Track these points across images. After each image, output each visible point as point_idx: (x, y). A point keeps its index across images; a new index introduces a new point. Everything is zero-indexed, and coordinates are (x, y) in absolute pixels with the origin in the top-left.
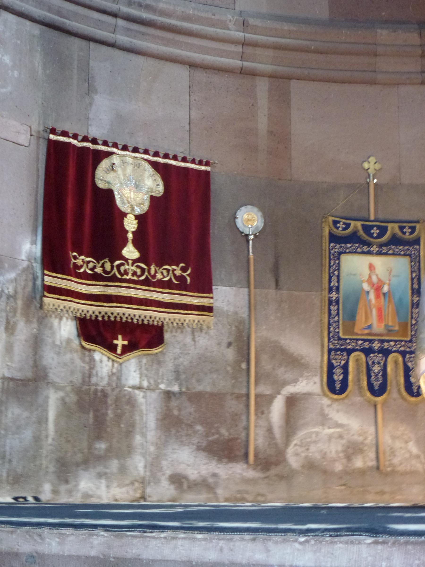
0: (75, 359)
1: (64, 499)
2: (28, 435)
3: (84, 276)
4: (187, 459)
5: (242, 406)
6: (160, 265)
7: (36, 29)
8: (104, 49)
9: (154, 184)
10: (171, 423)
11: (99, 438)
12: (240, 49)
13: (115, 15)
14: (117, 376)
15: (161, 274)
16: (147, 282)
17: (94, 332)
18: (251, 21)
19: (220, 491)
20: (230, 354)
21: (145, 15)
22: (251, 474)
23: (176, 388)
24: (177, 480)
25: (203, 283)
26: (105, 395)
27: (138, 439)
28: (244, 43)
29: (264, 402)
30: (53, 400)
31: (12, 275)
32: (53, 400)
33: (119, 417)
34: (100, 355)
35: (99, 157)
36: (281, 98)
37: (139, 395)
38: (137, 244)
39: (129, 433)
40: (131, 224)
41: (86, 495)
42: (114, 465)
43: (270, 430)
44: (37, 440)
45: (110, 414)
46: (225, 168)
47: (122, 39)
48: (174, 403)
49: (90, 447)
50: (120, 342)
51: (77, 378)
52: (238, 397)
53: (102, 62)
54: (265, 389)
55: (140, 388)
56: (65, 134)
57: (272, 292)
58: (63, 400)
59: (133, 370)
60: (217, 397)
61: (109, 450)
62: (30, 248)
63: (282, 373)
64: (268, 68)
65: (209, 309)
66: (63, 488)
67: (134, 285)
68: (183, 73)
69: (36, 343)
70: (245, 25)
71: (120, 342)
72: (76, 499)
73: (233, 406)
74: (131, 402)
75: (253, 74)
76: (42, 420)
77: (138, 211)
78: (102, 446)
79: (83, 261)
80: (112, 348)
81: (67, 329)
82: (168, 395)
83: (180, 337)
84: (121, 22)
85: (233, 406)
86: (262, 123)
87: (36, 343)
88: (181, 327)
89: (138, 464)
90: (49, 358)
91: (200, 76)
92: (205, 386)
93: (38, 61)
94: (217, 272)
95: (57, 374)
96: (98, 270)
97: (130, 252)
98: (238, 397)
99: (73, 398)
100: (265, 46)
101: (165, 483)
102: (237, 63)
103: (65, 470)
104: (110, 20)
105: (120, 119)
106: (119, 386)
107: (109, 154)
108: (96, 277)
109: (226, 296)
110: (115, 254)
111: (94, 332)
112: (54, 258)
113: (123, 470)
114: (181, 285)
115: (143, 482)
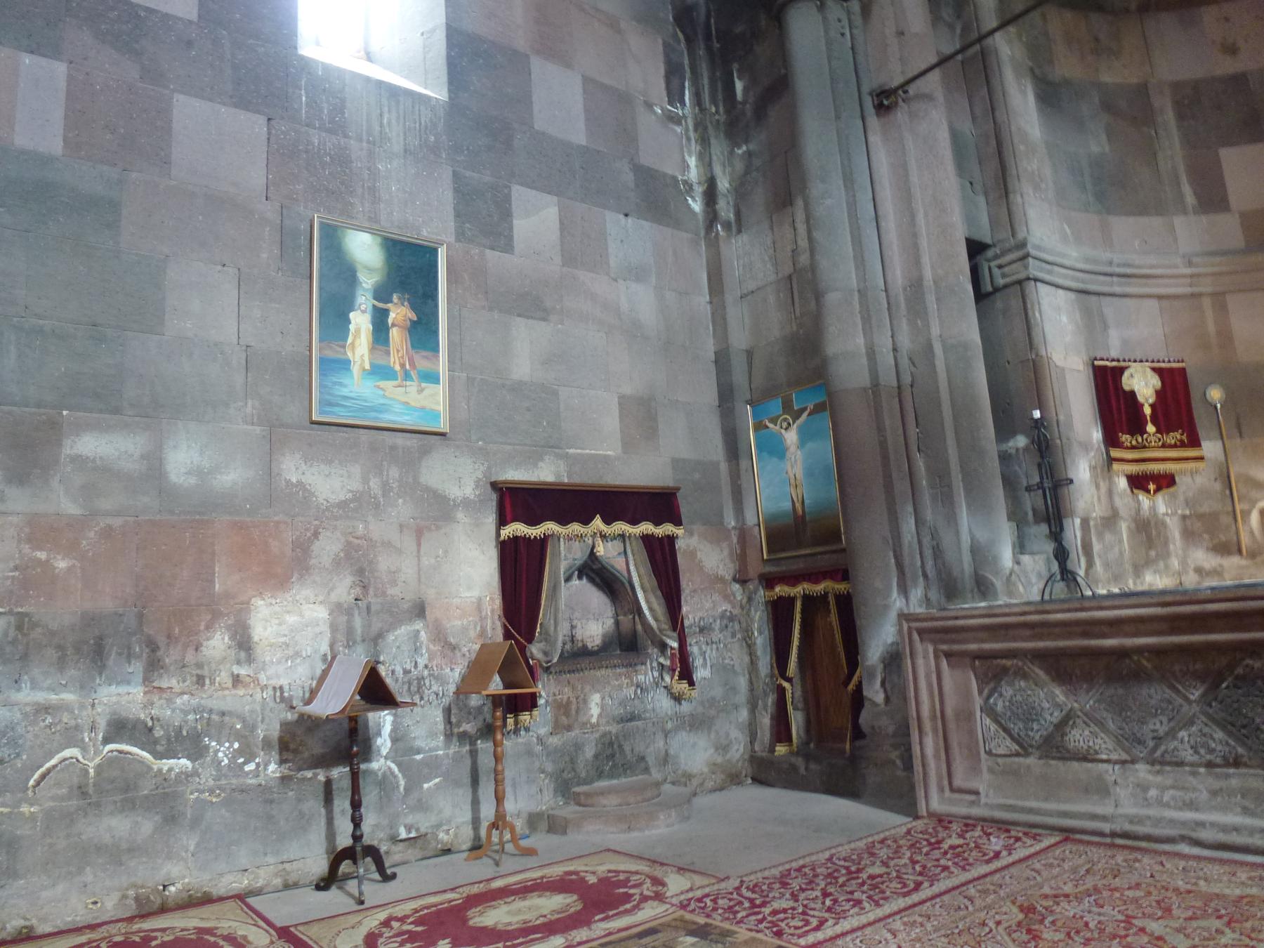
0: (1128, 499)
1: (1140, 588)
2: (1116, 550)
3: (1127, 448)
4: (1202, 557)
5: (1230, 519)
6: (1168, 433)
7: (1072, 295)
8: (1108, 299)
9: (1156, 382)
10: (1189, 535)
11: (1150, 548)
12: (1189, 280)
13: (1111, 275)
14: (1153, 508)
15: (1172, 438)
16: (1164, 446)
17: (1138, 482)
18: (1195, 260)
19: (1227, 576)
20: (1218, 486)
21: (1129, 271)
22: (1244, 562)
23: (1188, 512)
24: (1199, 570)
25: (1194, 442)
26: (1149, 522)
27: (1171, 547)
28: (1192, 276)
29: (1246, 514)
30: (1124, 527)
31: (1092, 454)
32: (1124, 527)
33: (1159, 534)
34: (1142, 497)
35: (1121, 370)
36: (1221, 307)
37: (1168, 519)
38: (1154, 423)
39: (1166, 543)
40: (1147, 411)
41: (1150, 585)
42: (1161, 564)
43: (1252, 532)
44: (1121, 553)
45: (1154, 532)
46: (1192, 362)
47: (1117, 289)
48: (1188, 522)
49: (1147, 554)
50: (1152, 487)
51: (1133, 513)
52: (1228, 513)
53: (1109, 308)
54: (1245, 506)
55: (1167, 514)
56: (1102, 359)
57: (1238, 440)
58: (1129, 527)
59: (1158, 504)
60: (1214, 516)
61: (1157, 555)
62: (1097, 435)
63: (1254, 494)
64: (1209, 289)
65: (1202, 458)
66: (1138, 581)
67: (1156, 449)
68: (1154, 303)
69: (1110, 493)
70: (1190, 264)
71: (1152, 487)
72: (1145, 587)
73: (1226, 520)
74: (1164, 524)
75: (1200, 295)
76: (1121, 541)
77: (1151, 401)
78: (1153, 553)
79: (1125, 438)
80: (1148, 491)
81: (1122, 483)
82: (1184, 517)
83: (1184, 479)
84: (1115, 279)
85: (1226, 520)
86: (1211, 328)
87: (1110, 493)
88: (1182, 472)
89: (1175, 563)
90: (1118, 502)
91: (1165, 303)
92: (1205, 508)
93: (1078, 316)
94: (1201, 433)
95: (1123, 512)
96: (1134, 443)
97: (1151, 428)
98: (1228, 513)
99: (1133, 525)
100: (1206, 275)
101: (1191, 573)
102: (1188, 290)
103: (1138, 570)
104: (1108, 279)
105: (1125, 343)
106: (1155, 514)
107: (1127, 368)
108: (1133, 448)
109: (1210, 448)
110: (1142, 431)
111: (1138, 482)
112: (1111, 440)
113: (1167, 567)
114: (1182, 445)
115: (1179, 574)
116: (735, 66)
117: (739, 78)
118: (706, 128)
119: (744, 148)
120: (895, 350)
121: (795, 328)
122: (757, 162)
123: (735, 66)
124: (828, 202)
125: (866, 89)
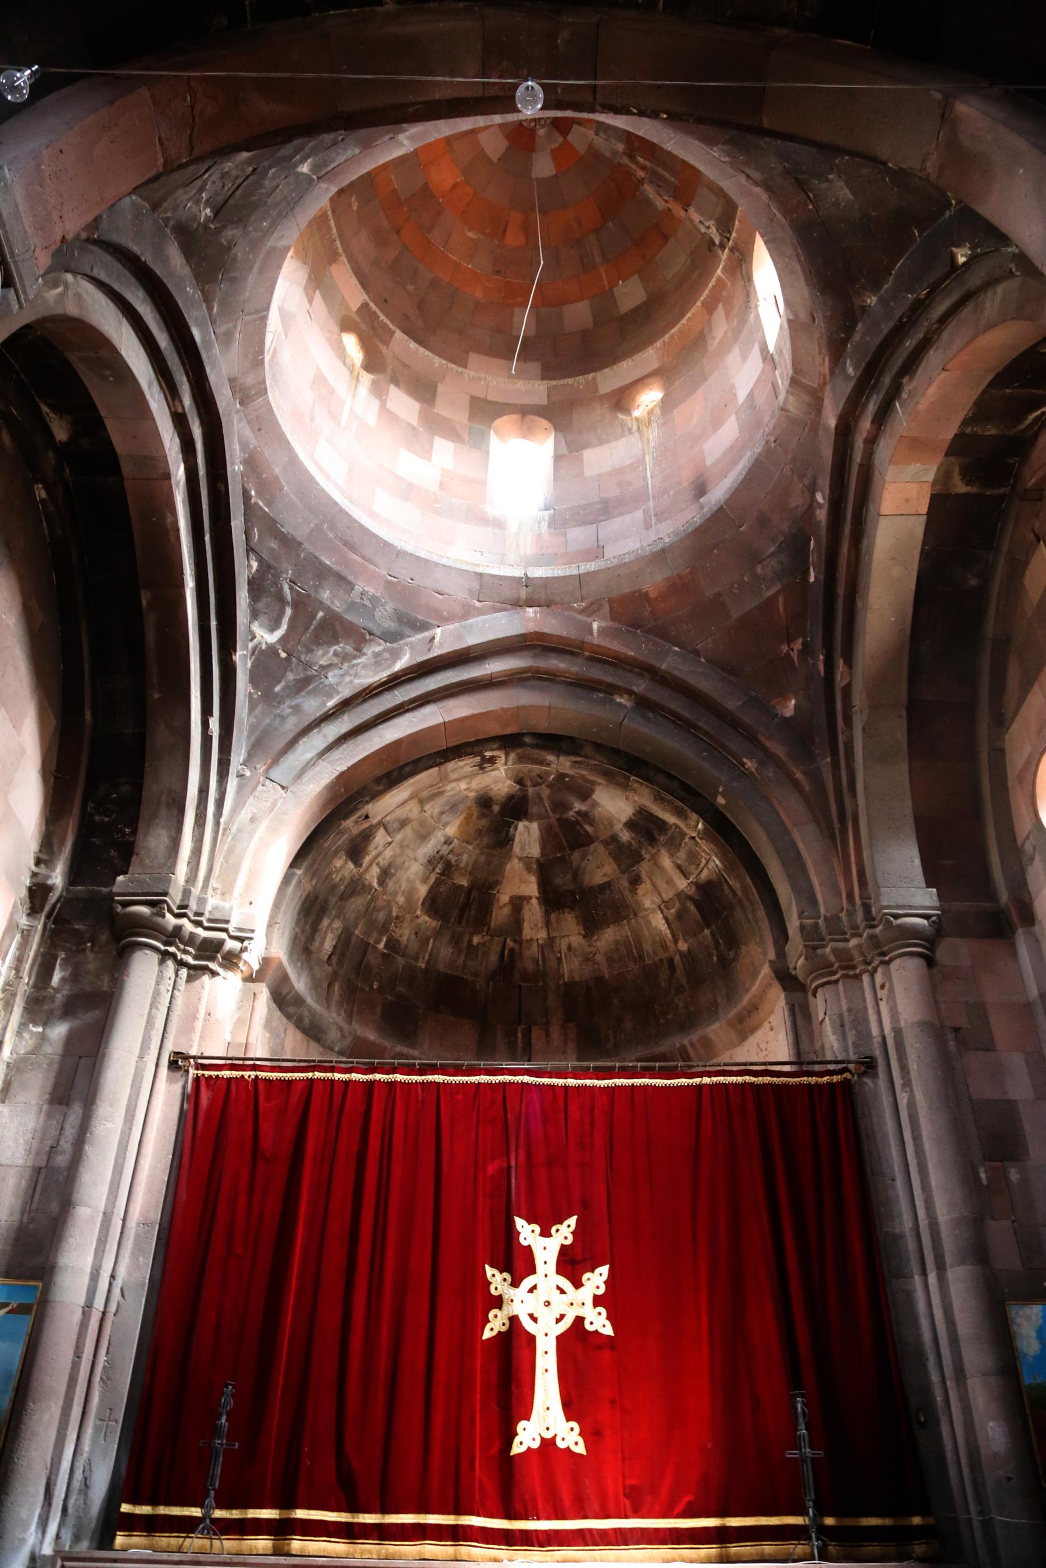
116: (62, 955)
117: (62, 969)
118: (14, 995)
119: (40, 1029)
120: (113, 1277)
121: (25, 1220)
122: (48, 1049)
123: (62, 955)
124: (109, 1125)
125: (170, 1047)
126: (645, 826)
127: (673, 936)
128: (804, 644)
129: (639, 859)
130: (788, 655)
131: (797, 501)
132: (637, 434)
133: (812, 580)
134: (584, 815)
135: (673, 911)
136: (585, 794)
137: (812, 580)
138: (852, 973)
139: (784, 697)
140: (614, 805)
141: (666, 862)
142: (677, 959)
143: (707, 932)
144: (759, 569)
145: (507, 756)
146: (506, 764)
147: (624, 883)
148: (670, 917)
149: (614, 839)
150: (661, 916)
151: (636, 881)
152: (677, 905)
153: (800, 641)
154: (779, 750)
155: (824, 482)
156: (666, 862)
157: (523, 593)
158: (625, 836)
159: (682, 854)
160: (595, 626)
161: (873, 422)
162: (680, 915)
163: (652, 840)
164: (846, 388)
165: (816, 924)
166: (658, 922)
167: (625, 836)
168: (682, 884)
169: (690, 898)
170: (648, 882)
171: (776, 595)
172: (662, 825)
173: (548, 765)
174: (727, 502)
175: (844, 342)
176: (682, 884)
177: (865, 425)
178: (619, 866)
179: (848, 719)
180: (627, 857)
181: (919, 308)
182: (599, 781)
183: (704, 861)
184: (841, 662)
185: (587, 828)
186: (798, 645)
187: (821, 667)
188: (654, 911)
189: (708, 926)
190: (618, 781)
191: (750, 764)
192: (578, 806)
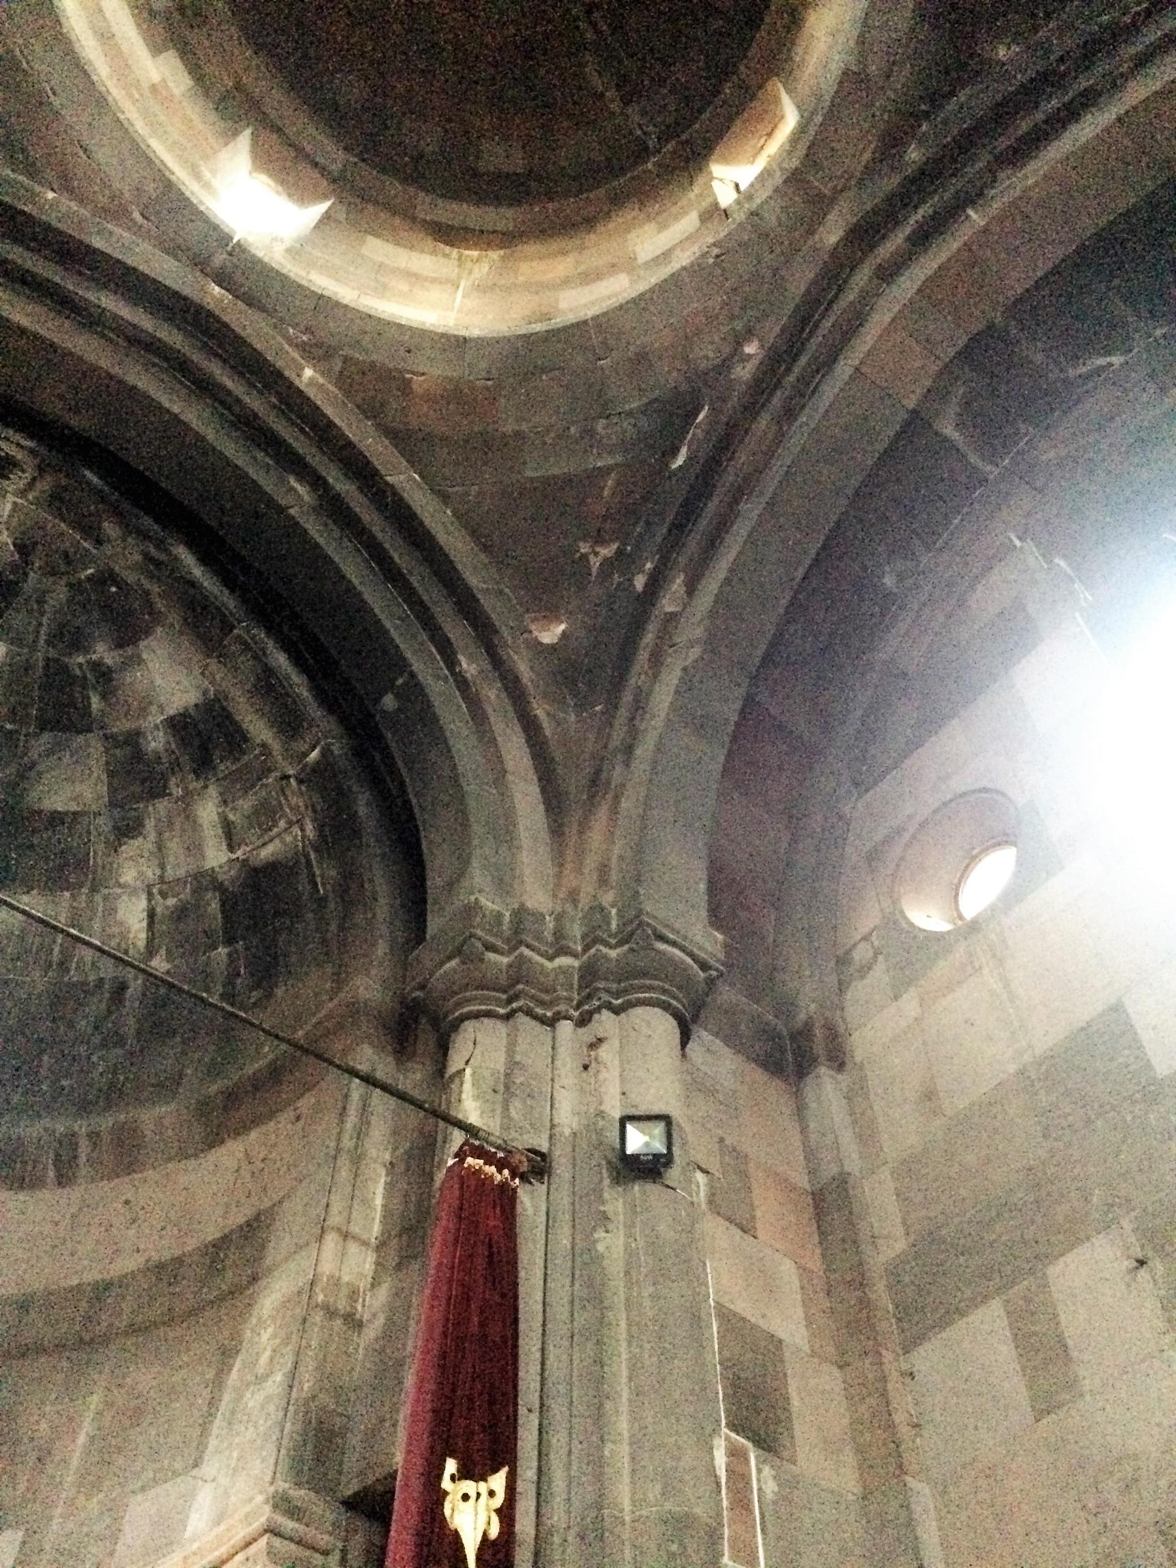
126: (206, 738)
127: (150, 941)
128: (620, 553)
129: (157, 791)
130: (584, 557)
131: (707, 352)
132: (456, 263)
133: (680, 461)
134: (104, 675)
135: (171, 901)
136: (128, 631)
137: (680, 461)
138: (539, 1011)
139: (551, 613)
140: (167, 679)
141: (208, 811)
142: (136, 985)
143: (222, 951)
144: (600, 425)
145: (41, 469)
146: (23, 493)
147: (104, 824)
148: (159, 910)
149: (133, 739)
150: (143, 903)
151: (127, 829)
152: (186, 894)
153: (615, 546)
154: (523, 668)
155: (773, 329)
156: (208, 811)
157: (219, 259)
158: (157, 742)
159: (246, 804)
160: (308, 373)
161: (908, 239)
162: (181, 913)
163: (203, 765)
164: (891, 183)
165: (499, 915)
166: (133, 917)
167: (157, 742)
168: (216, 856)
169: (219, 887)
170: (152, 837)
171: (608, 470)
172: (237, 740)
173: (99, 542)
174: (595, 318)
175: (919, 116)
176: (216, 856)
177: (896, 241)
178: (112, 790)
179: (656, 660)
180: (138, 779)
181: (1118, 34)
182: (174, 618)
183: (282, 824)
184: (680, 580)
185: (96, 703)
186: (606, 551)
187: (640, 582)
188: (134, 892)
189: (230, 941)
190: (205, 628)
191: (468, 666)
192: (103, 652)
